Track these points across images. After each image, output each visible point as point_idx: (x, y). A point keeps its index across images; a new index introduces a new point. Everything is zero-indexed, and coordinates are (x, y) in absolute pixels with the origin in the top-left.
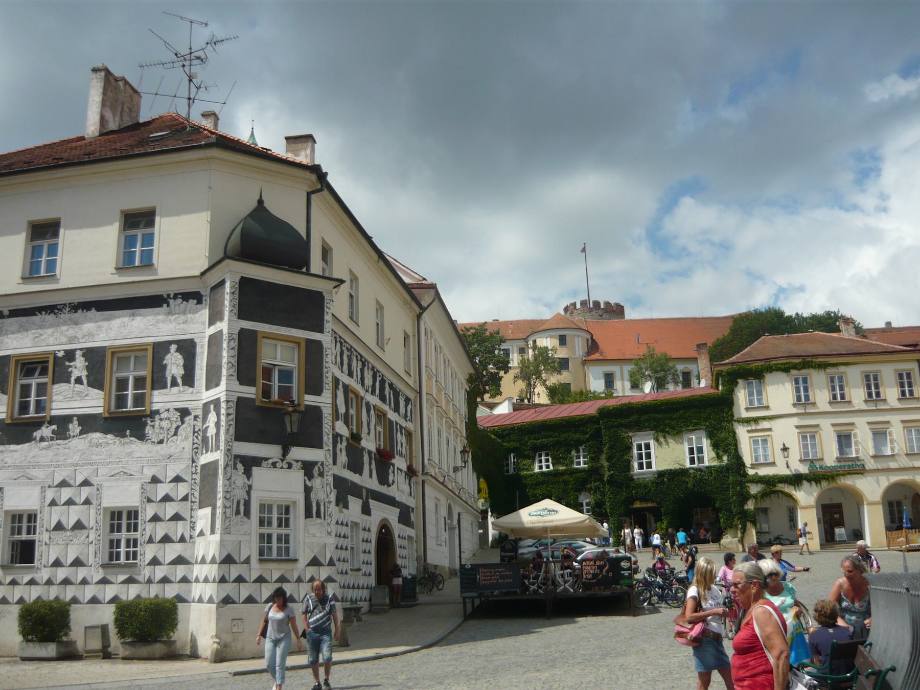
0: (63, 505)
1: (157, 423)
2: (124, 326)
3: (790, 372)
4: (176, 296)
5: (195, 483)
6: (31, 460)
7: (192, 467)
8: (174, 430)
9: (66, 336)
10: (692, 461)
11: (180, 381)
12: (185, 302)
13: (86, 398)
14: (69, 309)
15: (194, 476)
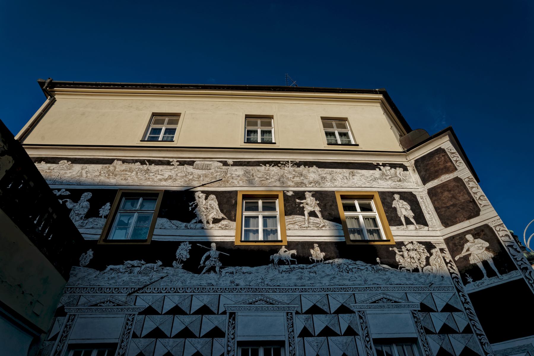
0: (319, 335)
1: (406, 254)
2: (347, 179)
4: (384, 165)
5: (471, 313)
6: (270, 283)
7: (460, 296)
8: (425, 260)
9: (293, 181)
11: (413, 220)
12: (393, 169)
13: (324, 228)
14: (292, 165)
15: (467, 306)
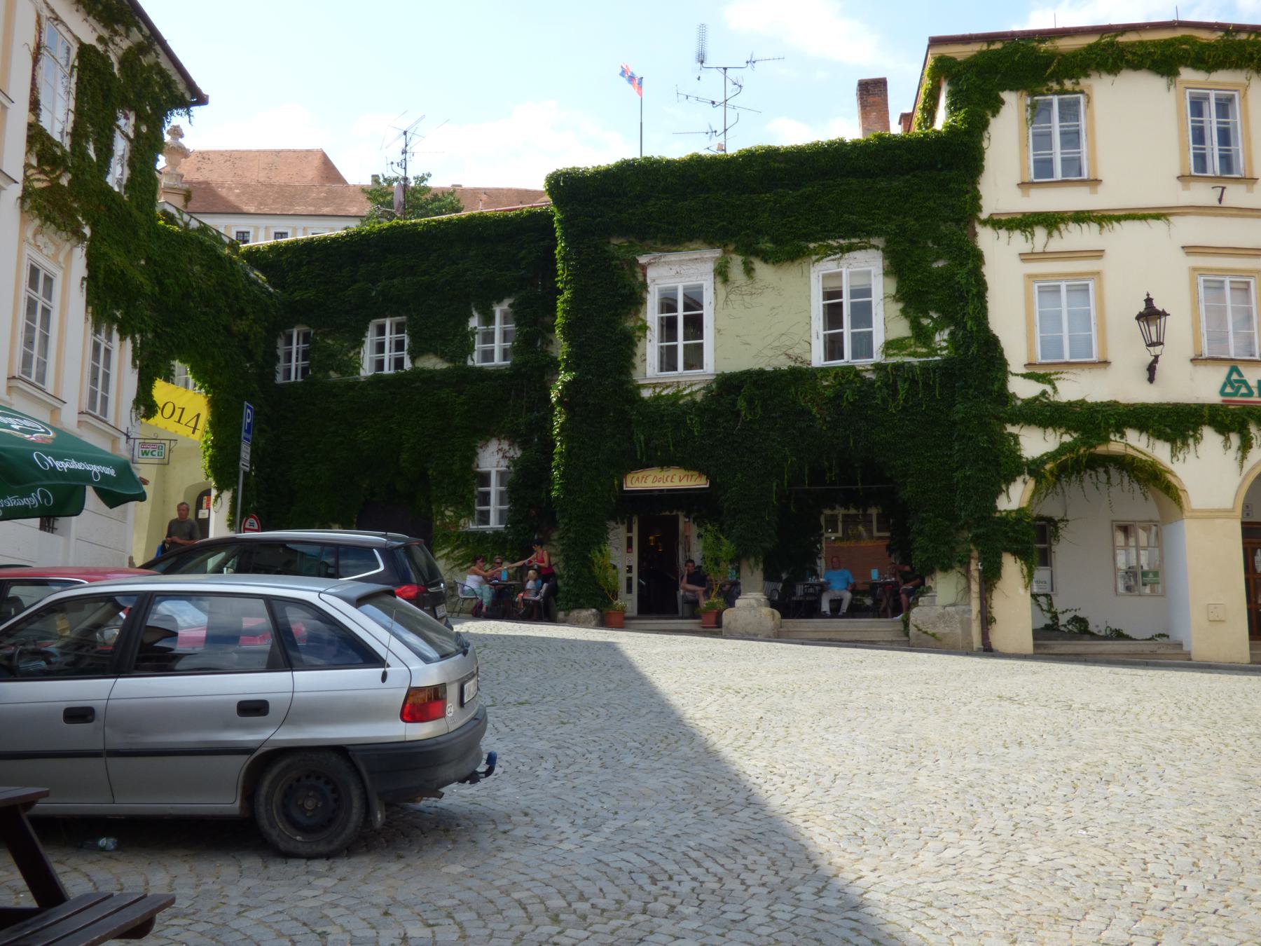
3: (1177, 74)
10: (834, 347)
